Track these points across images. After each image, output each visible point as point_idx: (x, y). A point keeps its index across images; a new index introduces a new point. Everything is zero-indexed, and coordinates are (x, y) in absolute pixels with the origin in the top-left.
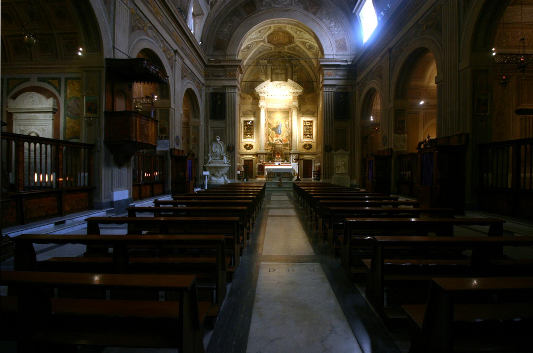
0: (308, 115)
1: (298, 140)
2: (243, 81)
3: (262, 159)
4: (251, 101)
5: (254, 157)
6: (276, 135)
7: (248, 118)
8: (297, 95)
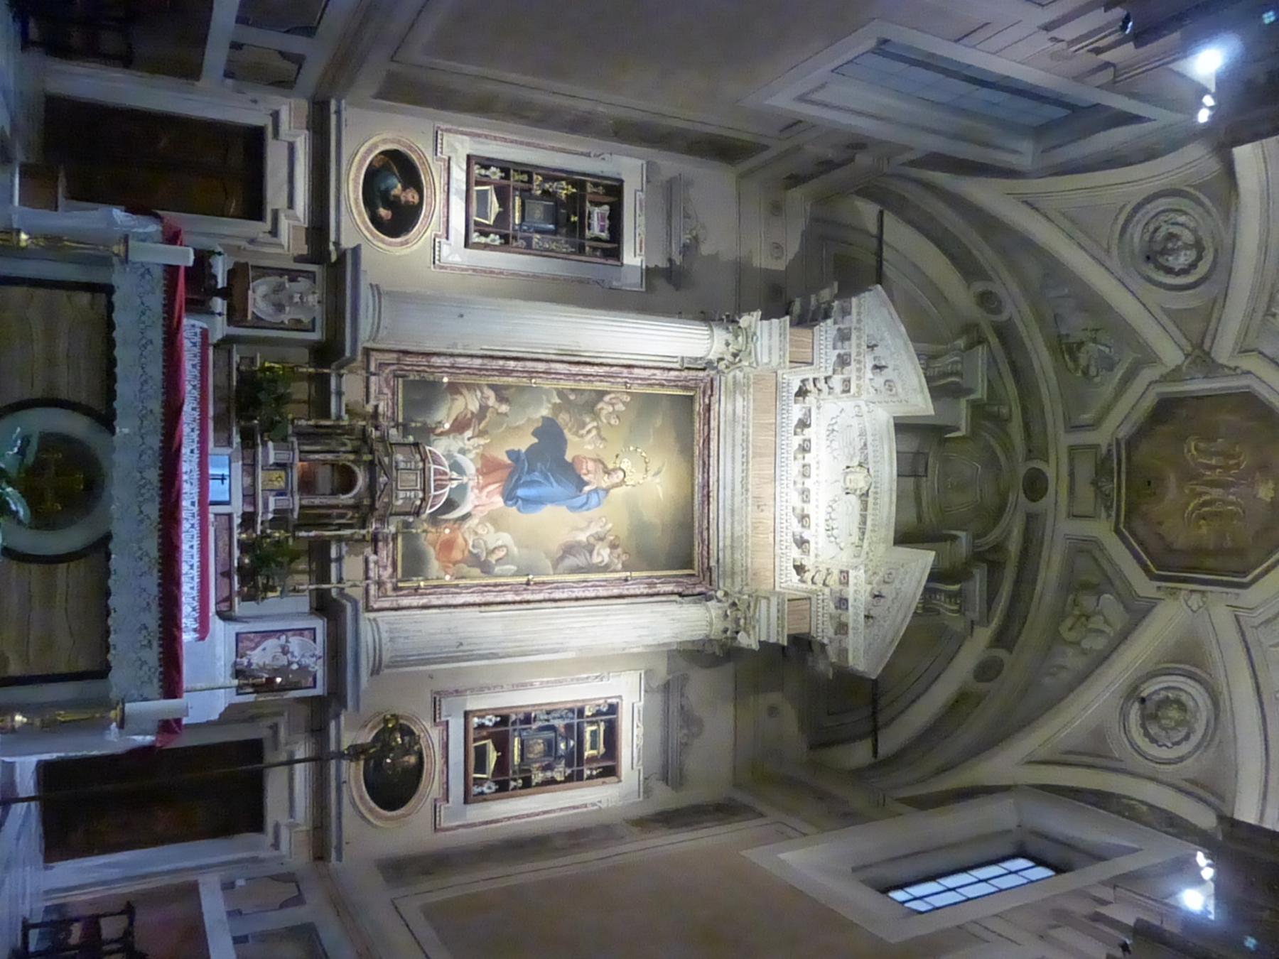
0: (657, 734)
2: (881, 213)
3: (279, 307)
4: (763, 260)
6: (505, 459)
7: (641, 220)
8: (824, 631)
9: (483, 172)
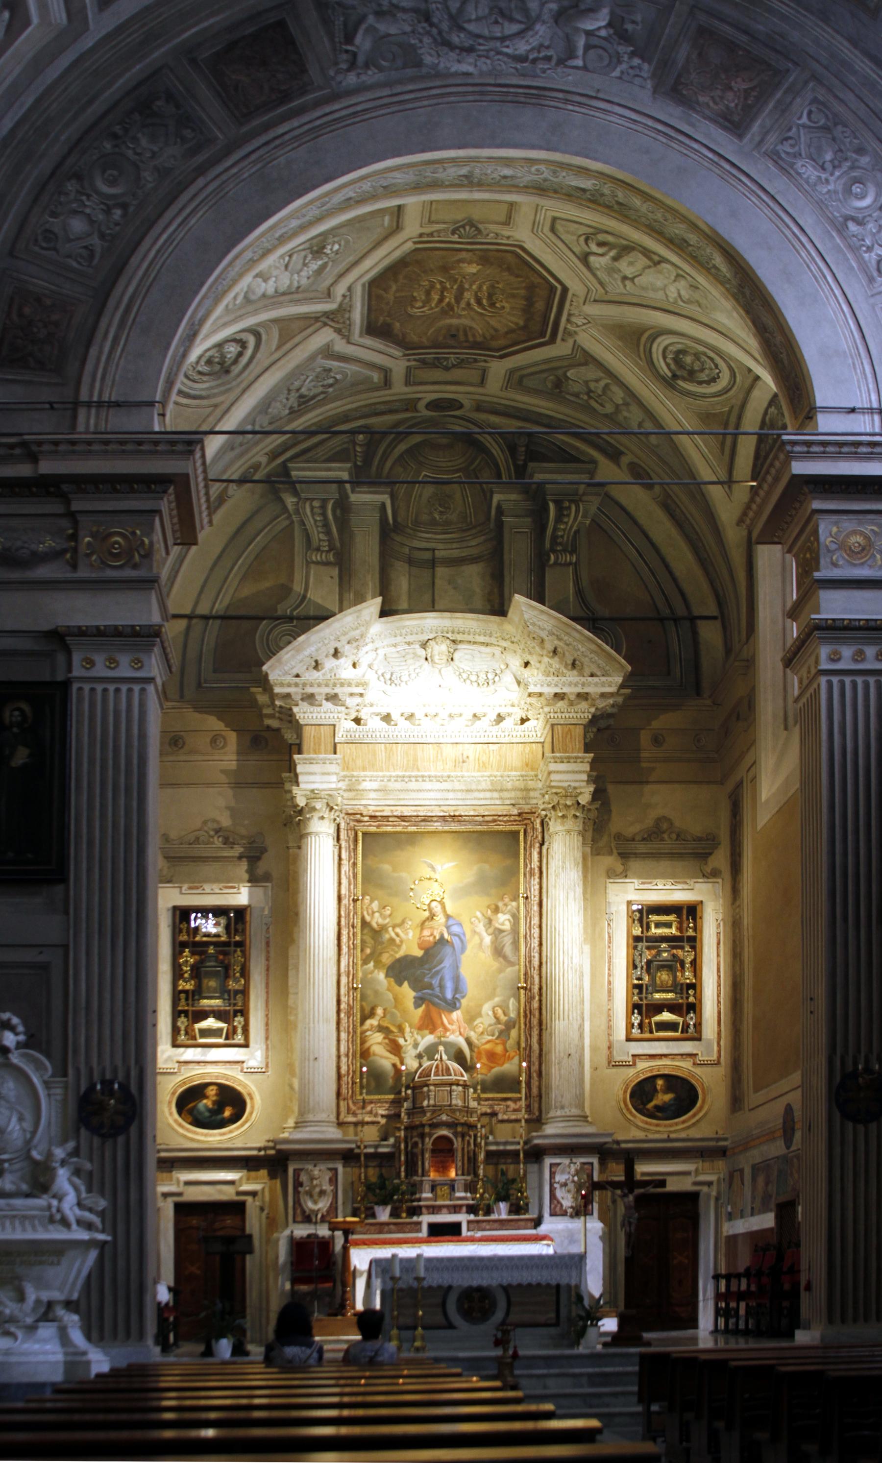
0: (665, 865)
1: (594, 1049)
5: (256, 1180)
6: (421, 1010)
7: (207, 888)
9: (183, 1032)
